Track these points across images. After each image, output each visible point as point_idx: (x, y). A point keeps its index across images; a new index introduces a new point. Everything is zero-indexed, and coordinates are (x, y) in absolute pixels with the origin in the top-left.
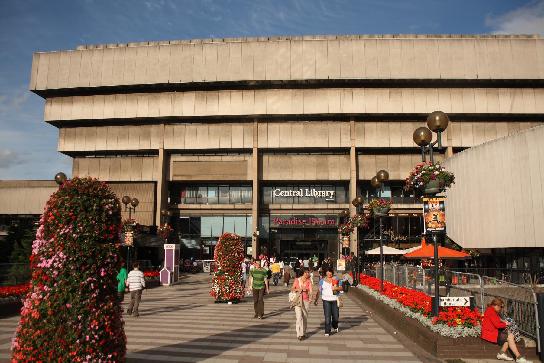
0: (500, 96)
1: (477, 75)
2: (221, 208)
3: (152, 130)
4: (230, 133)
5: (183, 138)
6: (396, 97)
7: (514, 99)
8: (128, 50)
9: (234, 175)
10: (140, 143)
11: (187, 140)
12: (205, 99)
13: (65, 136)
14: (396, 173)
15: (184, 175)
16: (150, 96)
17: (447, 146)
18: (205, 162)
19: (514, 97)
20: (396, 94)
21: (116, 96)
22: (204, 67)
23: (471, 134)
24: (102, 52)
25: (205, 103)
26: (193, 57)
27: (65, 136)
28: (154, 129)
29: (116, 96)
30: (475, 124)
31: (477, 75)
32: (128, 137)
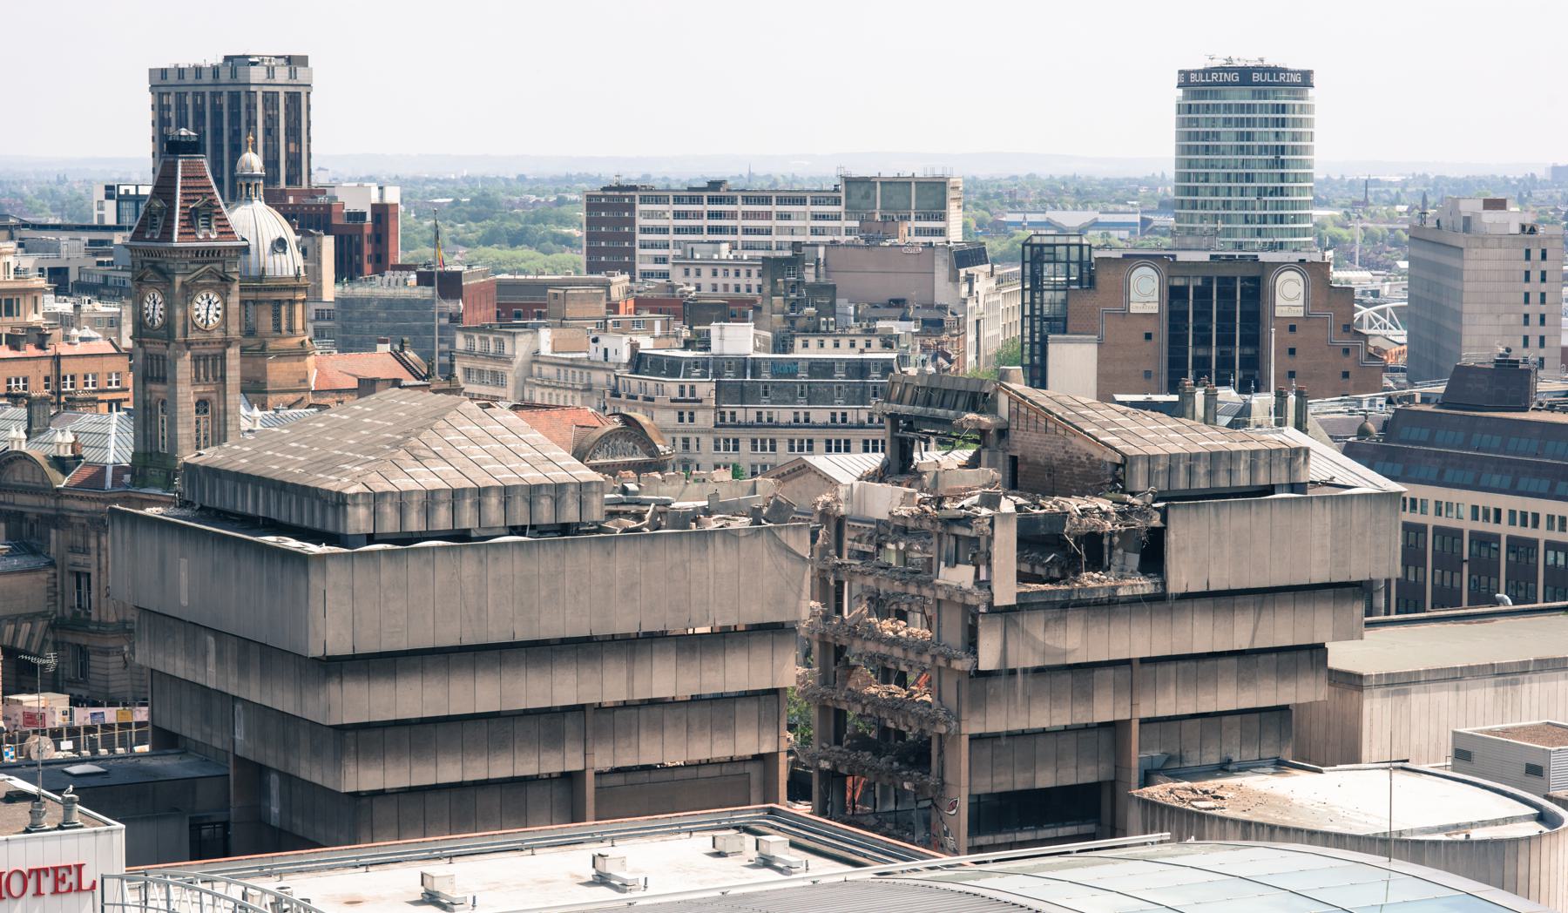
3: (567, 724)
4: (732, 722)
5: (634, 740)
10: (541, 758)
11: (643, 746)
12: (698, 655)
13: (357, 753)
14: (1028, 775)
19: (1259, 615)
21: (500, 653)
22: (711, 591)
23: (1172, 688)
24: (483, 552)
25: (697, 663)
26: (688, 564)
27: (357, 753)
29: (500, 653)
32: (511, 745)
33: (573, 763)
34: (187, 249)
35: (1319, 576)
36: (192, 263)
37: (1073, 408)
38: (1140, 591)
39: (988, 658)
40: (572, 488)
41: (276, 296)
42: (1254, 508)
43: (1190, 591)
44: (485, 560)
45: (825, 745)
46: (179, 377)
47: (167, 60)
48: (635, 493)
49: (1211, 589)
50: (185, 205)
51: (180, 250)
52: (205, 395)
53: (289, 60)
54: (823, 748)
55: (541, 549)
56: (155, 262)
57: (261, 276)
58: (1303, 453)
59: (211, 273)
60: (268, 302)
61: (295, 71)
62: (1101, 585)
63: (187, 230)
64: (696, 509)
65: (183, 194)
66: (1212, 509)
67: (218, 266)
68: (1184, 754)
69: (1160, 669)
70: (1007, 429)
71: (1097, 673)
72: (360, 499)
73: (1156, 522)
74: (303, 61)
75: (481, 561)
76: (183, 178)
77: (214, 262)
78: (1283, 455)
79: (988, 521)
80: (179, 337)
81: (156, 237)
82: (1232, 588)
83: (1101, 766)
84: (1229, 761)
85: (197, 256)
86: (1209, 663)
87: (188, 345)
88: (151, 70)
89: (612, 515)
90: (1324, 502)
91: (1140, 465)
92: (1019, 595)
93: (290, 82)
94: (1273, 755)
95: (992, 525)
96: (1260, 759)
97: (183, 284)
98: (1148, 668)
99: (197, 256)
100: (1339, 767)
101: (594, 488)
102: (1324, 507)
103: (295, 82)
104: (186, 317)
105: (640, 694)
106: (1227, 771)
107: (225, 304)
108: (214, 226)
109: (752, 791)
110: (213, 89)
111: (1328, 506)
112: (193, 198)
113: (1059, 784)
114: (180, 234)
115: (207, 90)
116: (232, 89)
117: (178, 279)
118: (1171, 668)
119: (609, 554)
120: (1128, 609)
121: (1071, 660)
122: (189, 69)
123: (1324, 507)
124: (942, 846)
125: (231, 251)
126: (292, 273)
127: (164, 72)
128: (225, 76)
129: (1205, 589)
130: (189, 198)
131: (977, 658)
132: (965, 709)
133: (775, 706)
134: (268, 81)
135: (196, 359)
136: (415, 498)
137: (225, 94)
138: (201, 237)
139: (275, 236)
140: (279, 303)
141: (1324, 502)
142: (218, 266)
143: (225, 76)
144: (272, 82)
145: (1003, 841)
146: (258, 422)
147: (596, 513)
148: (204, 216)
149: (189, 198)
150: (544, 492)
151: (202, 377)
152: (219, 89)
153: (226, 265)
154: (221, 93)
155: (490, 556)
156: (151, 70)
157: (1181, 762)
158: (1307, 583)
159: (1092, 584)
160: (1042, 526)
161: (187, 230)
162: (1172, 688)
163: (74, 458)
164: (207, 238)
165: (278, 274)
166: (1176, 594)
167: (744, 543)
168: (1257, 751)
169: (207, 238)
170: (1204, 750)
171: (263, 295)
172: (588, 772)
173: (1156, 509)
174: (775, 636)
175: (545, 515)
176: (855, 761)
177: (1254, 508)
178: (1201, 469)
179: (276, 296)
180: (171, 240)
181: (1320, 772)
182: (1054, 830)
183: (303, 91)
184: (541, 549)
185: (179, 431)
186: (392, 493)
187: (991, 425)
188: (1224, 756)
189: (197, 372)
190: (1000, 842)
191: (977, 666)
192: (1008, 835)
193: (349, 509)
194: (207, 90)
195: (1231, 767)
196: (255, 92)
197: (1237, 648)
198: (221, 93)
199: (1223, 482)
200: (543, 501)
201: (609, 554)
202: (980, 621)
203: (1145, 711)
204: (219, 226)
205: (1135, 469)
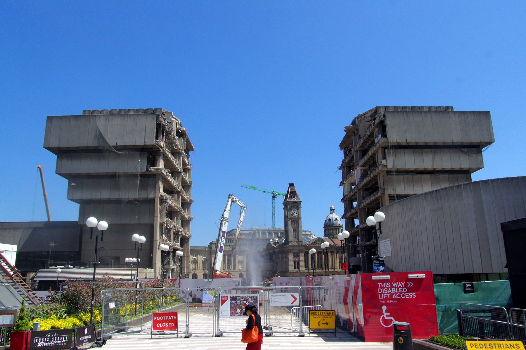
1: (406, 140)
8: (130, 116)
23: (402, 184)
30: (406, 176)
31: (406, 140)
36: (291, 204)
41: (336, 228)
46: (289, 224)
51: (289, 201)
52: (295, 228)
55: (129, 117)
57: (333, 225)
58: (450, 108)
67: (297, 205)
80: (289, 217)
87: (291, 218)
90: (455, 114)
91: (381, 109)
97: (289, 208)
102: (455, 115)
104: (290, 213)
108: (296, 198)
111: (457, 115)
114: (289, 199)
117: (288, 207)
123: (455, 115)
126: (339, 224)
135: (292, 221)
139: (335, 218)
140: (337, 229)
141: (455, 114)
151: (294, 224)
155: (109, 119)
162: (402, 184)
163: (277, 242)
165: (336, 224)
169: (294, 200)
171: (333, 228)
172: (156, 199)
179: (336, 228)
184: (129, 117)
185: (289, 234)
189: (293, 224)
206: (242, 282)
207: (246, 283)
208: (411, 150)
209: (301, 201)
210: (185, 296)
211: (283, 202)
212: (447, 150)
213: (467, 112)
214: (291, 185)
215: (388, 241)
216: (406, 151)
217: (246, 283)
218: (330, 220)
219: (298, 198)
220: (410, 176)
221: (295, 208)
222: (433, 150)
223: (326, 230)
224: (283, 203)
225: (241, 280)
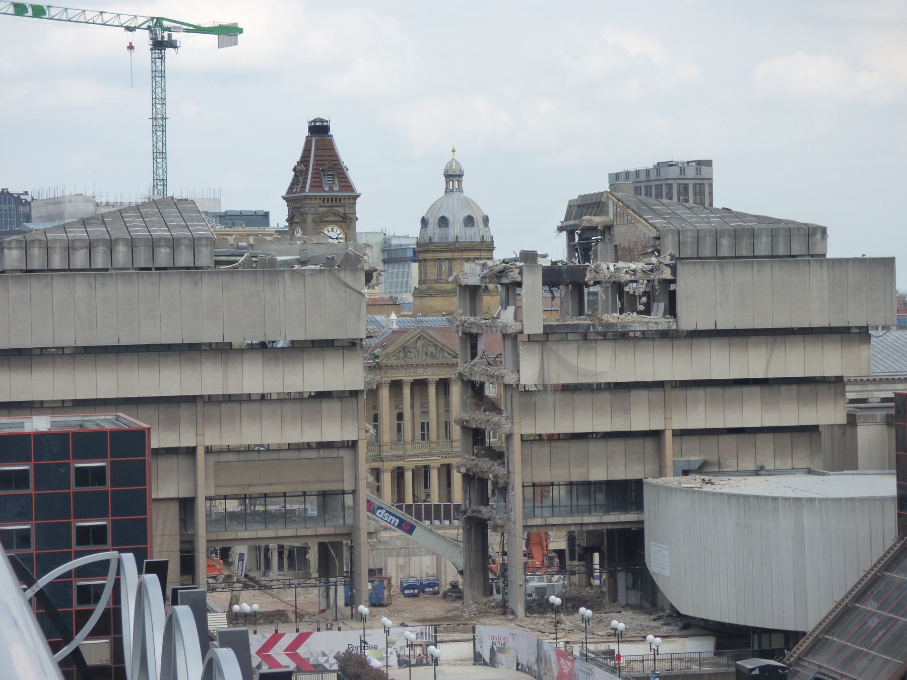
0: (749, 349)
1: (716, 324)
2: (293, 535)
6: (587, 357)
7: (772, 353)
9: (320, 481)
12: (281, 363)
15: (235, 486)
16: (182, 356)
17: (663, 428)
18: (270, 462)
20: (587, 350)
23: (701, 408)
24: (92, 279)
28: (184, 411)
30: (709, 390)
31: (716, 324)
33: (187, 441)
34: (316, 198)
35: (819, 321)
36: (321, 206)
37: (649, 206)
38: (653, 327)
39: (529, 374)
40: (187, 242)
42: (755, 266)
43: (699, 328)
44: (94, 285)
45: (467, 456)
47: (619, 168)
48: (244, 248)
49: (719, 328)
50: (316, 167)
51: (311, 198)
53: (699, 163)
54: (466, 458)
56: (299, 208)
59: (336, 214)
60: (460, 259)
61: (700, 170)
62: (620, 321)
63: (316, 184)
64: (291, 260)
65: (314, 160)
66: (717, 266)
67: (341, 210)
68: (722, 461)
69: (691, 393)
70: (612, 226)
71: (634, 393)
72: (14, 244)
73: (667, 274)
74: (709, 163)
75: (90, 286)
76: (315, 149)
77: (337, 206)
78: (802, 232)
79: (518, 271)
81: (298, 190)
82: (738, 328)
83: (647, 467)
84: (762, 468)
85: (324, 201)
86: (734, 391)
88: (610, 174)
89: (217, 263)
92: (545, 327)
93: (697, 177)
94: (806, 467)
95: (521, 273)
96: (793, 469)
98: (679, 392)
99: (324, 201)
100: (845, 472)
101: (204, 242)
102: (821, 267)
103: (700, 177)
105: (233, 389)
106: (759, 475)
107: (346, 235)
109: (345, 470)
110: (646, 184)
111: (825, 267)
112: (322, 163)
113: (610, 478)
114: (311, 186)
115: (643, 185)
116: (657, 183)
118: (700, 392)
119: (196, 284)
120: (651, 342)
121: (602, 380)
122: (632, 172)
123: (821, 267)
124: (510, 520)
125: (349, 198)
126: (478, 239)
127: (617, 175)
128: (653, 176)
129: (713, 328)
130: (319, 162)
131: (519, 375)
132: (516, 414)
133: (355, 405)
134: (681, 177)
136: (58, 245)
137: (653, 187)
138: (327, 189)
139: (466, 214)
141: (821, 265)
142: (341, 210)
143: (653, 176)
144: (684, 177)
145: (572, 522)
146: (394, 323)
147: (205, 258)
148: (328, 175)
149: (319, 162)
150: (163, 243)
152: (650, 184)
153: (346, 208)
154: (651, 186)
156: (610, 174)
157: (719, 467)
158: (807, 326)
159: (612, 320)
160: (565, 276)
161: (316, 184)
162: (701, 408)
164: (331, 190)
166: (687, 331)
167: (308, 279)
168: (790, 462)
170: (740, 461)
171: (456, 255)
173: (666, 265)
174: (345, 352)
175: (163, 256)
176: (476, 465)
177: (755, 266)
178: (725, 242)
180: (304, 191)
181: (828, 475)
182: (617, 516)
183: (706, 183)
186: (40, 241)
187: (599, 223)
188: (759, 464)
190: (569, 522)
191: (519, 380)
192: (576, 518)
193: (6, 251)
194: (643, 185)
195: (761, 472)
196: (672, 184)
197: (752, 377)
198: (651, 186)
199: (744, 251)
200: (163, 250)
201: (196, 284)
202: (520, 347)
203: (679, 423)
204: (341, 182)
205: (666, 240)
206: (422, 633)
207: (429, 634)
208: (725, 340)
209: (358, 196)
210: (327, 661)
211: (284, 193)
212: (799, 338)
213: (848, 260)
214: (319, 130)
215: (667, 549)
216: (715, 342)
217: (429, 634)
218: (443, 222)
219: (347, 185)
220: (718, 391)
221: (334, 222)
222: (770, 339)
223: (429, 264)
224: (284, 198)
225: (421, 629)
